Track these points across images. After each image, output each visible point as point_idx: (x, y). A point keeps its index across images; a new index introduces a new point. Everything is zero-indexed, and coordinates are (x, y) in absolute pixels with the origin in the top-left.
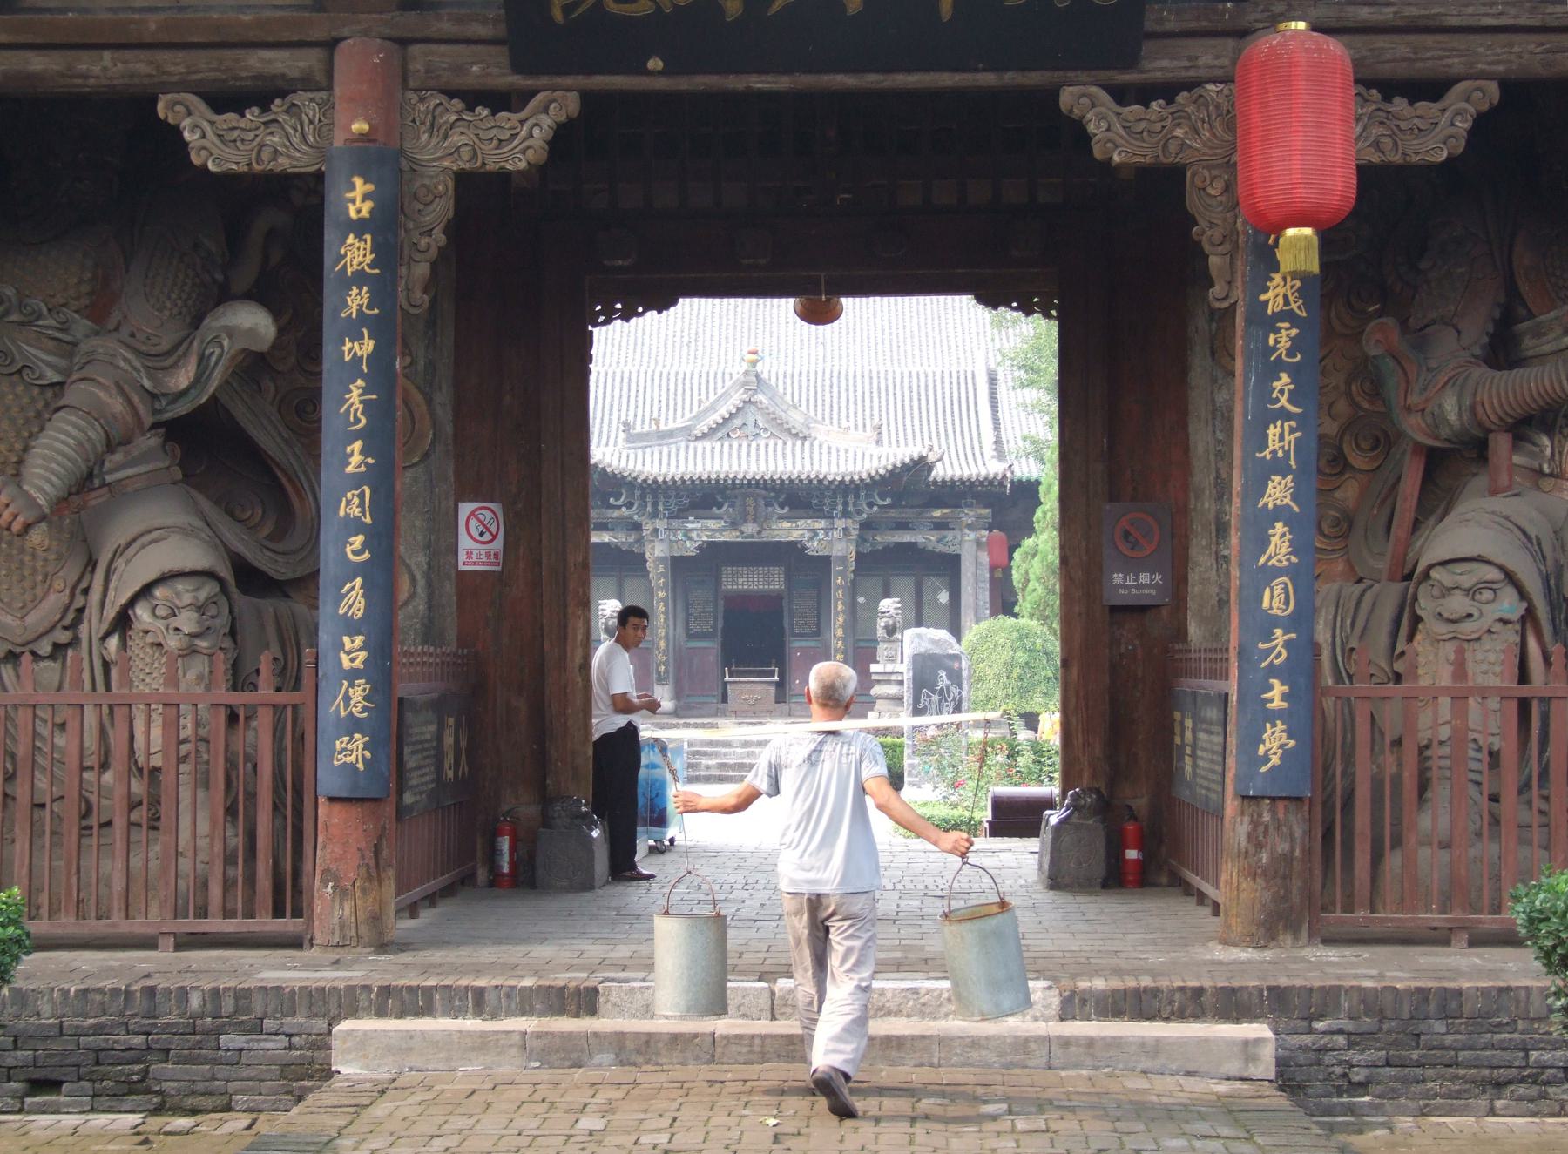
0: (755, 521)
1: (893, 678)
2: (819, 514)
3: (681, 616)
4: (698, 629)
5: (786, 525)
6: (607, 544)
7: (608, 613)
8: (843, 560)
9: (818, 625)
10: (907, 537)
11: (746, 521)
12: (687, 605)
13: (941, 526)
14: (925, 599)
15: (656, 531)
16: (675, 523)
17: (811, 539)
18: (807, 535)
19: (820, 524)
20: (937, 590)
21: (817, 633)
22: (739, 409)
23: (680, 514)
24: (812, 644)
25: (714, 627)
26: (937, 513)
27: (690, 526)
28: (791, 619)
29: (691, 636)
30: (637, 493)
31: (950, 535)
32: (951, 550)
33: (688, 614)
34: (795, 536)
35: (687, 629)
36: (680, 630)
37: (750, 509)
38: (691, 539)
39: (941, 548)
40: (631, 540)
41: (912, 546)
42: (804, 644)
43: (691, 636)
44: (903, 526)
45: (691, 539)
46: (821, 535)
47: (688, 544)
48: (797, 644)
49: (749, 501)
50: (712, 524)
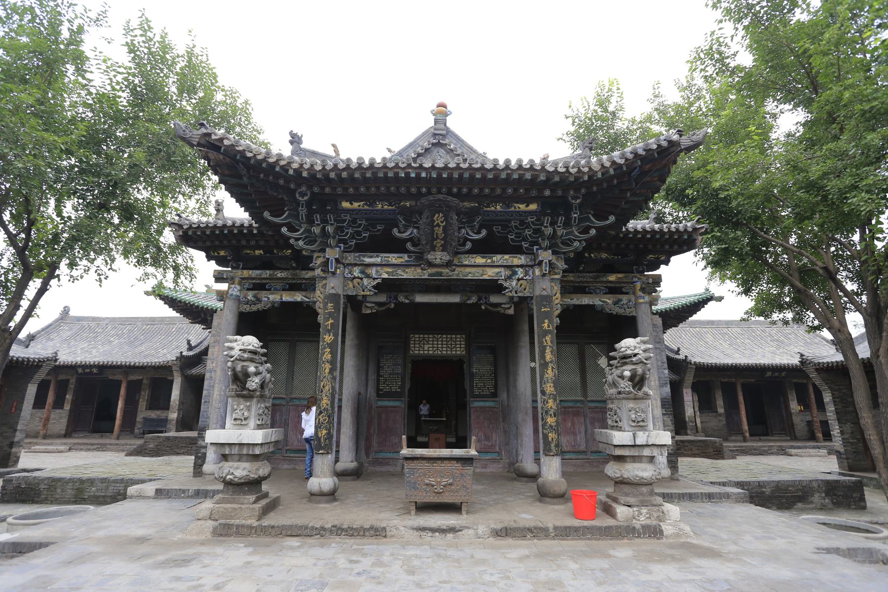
0: (444, 249)
1: (646, 452)
2: (517, 250)
3: (372, 377)
4: (387, 389)
5: (480, 260)
8: (547, 299)
9: (496, 387)
10: (586, 300)
11: (433, 249)
12: (379, 368)
13: (614, 290)
14: (587, 364)
15: (326, 263)
16: (351, 258)
17: (509, 278)
18: (504, 273)
20: (597, 357)
21: (495, 395)
22: (427, 150)
23: (362, 248)
24: (488, 404)
25: (402, 387)
26: (612, 278)
27: (368, 260)
28: (472, 382)
29: (380, 395)
30: (303, 211)
31: (624, 299)
32: (629, 312)
33: (379, 376)
34: (490, 274)
35: (378, 390)
36: (371, 391)
37: (439, 231)
38: (368, 276)
39: (616, 310)
41: (592, 307)
42: (481, 404)
43: (380, 395)
44: (582, 290)
45: (368, 276)
46: (520, 273)
47: (365, 281)
48: (476, 404)
49: (438, 218)
50: (393, 258)
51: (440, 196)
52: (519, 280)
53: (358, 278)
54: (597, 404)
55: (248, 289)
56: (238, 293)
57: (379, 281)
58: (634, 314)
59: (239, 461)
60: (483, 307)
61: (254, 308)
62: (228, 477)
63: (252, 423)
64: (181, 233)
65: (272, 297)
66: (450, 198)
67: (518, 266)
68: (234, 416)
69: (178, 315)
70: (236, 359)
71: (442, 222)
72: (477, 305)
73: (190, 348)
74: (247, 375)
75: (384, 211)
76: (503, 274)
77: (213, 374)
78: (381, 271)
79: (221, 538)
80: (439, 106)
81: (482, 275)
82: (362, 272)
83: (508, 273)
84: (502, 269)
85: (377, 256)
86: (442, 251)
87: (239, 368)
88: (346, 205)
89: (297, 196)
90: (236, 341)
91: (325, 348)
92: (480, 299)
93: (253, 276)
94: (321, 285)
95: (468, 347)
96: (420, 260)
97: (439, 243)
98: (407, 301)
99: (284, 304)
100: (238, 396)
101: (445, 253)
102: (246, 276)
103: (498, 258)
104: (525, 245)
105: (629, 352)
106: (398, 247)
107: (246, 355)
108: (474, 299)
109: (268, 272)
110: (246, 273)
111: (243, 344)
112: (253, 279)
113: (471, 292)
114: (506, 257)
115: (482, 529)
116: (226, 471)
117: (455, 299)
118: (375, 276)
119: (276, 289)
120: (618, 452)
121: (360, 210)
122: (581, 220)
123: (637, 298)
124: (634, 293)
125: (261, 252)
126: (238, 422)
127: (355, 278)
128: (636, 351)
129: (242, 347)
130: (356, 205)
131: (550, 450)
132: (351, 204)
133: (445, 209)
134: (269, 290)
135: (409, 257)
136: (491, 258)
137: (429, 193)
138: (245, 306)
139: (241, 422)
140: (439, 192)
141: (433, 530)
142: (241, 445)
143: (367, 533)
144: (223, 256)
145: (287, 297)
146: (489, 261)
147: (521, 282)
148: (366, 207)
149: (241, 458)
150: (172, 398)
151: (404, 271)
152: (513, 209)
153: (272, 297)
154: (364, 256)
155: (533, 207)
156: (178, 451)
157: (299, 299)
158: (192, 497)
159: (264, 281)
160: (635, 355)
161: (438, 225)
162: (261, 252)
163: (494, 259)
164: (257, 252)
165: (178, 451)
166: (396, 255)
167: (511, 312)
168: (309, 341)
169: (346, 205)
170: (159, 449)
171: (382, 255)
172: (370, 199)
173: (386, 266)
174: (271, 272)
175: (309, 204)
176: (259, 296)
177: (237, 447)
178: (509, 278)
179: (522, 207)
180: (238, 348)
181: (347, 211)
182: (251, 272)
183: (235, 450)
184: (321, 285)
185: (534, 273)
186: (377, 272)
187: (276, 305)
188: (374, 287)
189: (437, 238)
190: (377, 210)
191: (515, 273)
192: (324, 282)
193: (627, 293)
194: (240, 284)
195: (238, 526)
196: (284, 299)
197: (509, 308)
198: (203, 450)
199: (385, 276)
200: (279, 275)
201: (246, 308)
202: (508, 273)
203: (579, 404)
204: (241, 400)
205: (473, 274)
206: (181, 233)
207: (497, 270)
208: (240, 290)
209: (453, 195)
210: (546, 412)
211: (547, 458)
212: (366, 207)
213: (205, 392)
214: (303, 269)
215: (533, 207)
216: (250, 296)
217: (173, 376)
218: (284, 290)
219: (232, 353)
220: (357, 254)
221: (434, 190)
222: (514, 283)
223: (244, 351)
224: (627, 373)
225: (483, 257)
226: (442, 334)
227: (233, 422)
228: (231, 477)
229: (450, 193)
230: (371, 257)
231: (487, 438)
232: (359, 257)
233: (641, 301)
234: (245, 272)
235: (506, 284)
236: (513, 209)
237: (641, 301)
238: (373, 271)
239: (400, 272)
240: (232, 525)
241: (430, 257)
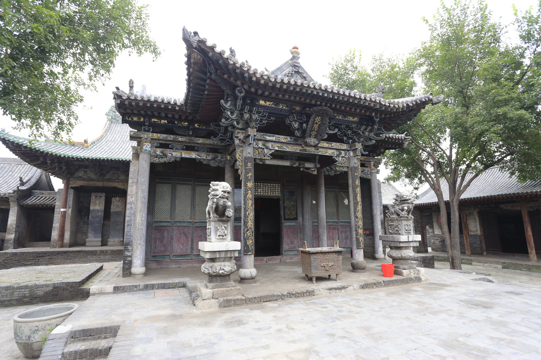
6: (194, 160)
7: (220, 193)
9: (297, 214)
17: (338, 156)
18: (336, 153)
19: (345, 147)
21: (296, 219)
27: (268, 138)
28: (284, 211)
30: (239, 103)
31: (366, 169)
34: (329, 153)
37: (316, 126)
38: (267, 148)
40: (209, 158)
42: (289, 224)
45: (267, 148)
47: (266, 151)
48: (286, 224)
49: (318, 119)
50: (282, 138)
51: (325, 108)
52: (342, 157)
53: (261, 148)
54: (343, 224)
55: (156, 147)
56: (150, 150)
57: (273, 151)
58: (370, 178)
59: (224, 261)
60: (301, 169)
61: (162, 160)
62: (221, 272)
63: (229, 237)
64: (119, 102)
65: (174, 154)
66: (329, 109)
67: (342, 150)
68: (218, 233)
69: (17, 157)
70: (220, 197)
72: (298, 168)
73: (22, 184)
74: (225, 207)
75: (282, 109)
76: (335, 153)
77: (133, 205)
78: (275, 146)
79: (225, 308)
80: (293, 48)
81: (326, 153)
82: (264, 145)
83: (338, 153)
84: (335, 151)
85: (273, 136)
86: (314, 138)
87: (221, 202)
88: (262, 102)
89: (237, 92)
90: (217, 185)
91: (248, 191)
92: (300, 165)
93: (161, 138)
94: (239, 150)
95: (282, 191)
96: (296, 141)
97: (314, 133)
98: (261, 163)
99: (182, 159)
100: (219, 221)
101: (315, 139)
102: (156, 137)
103: (335, 145)
104: (345, 138)
105: (408, 198)
106: (287, 131)
107: (226, 195)
108: (297, 165)
109: (172, 136)
110: (155, 136)
111: (223, 188)
112: (160, 140)
113: (296, 160)
114: (338, 144)
115: (356, 286)
116: (218, 268)
117: (287, 163)
118: (271, 148)
119: (177, 149)
120: (402, 245)
121: (269, 107)
122: (378, 129)
123: (371, 170)
124: (370, 167)
125: (166, 121)
126: (221, 237)
127: (259, 148)
128: (410, 198)
129: (224, 190)
130: (268, 103)
131: (360, 246)
132: (265, 102)
133: (322, 114)
134: (172, 149)
135: (291, 138)
136: (331, 144)
137: (320, 105)
138: (155, 159)
139: (222, 237)
140: (326, 106)
141: (336, 289)
142: (226, 251)
143: (305, 295)
144: (135, 121)
145: (186, 155)
147: (344, 158)
148: (273, 106)
149: (225, 259)
150: (9, 222)
151: (287, 147)
152: (346, 119)
153: (174, 154)
154: (266, 135)
155: (356, 119)
156: (26, 263)
157: (194, 157)
158: (142, 290)
159: (168, 142)
160: (410, 199)
161: (317, 123)
162: (166, 121)
163: (333, 145)
164: (163, 121)
165: (26, 263)
166: (284, 137)
167: (315, 173)
168: (185, 184)
169: (262, 102)
170: (6, 263)
171: (276, 136)
172: (277, 101)
173: (277, 142)
174: (174, 136)
175: (244, 99)
176: (165, 152)
177: (224, 253)
178: (338, 156)
179: (351, 119)
180: (221, 190)
181: (262, 106)
182: (159, 135)
183: (223, 255)
184: (239, 150)
185: (349, 153)
186: (272, 145)
187: (178, 159)
189: (314, 130)
190: (279, 109)
191: (341, 153)
192: (241, 149)
193: (367, 167)
194: (150, 143)
195: (235, 300)
196: (183, 156)
197: (314, 171)
198: (129, 259)
199: (277, 149)
200: (180, 139)
201: (157, 160)
202: (338, 153)
203: (335, 224)
204: (221, 223)
205: (322, 152)
206: (119, 102)
207: (332, 151)
208: (151, 147)
209: (332, 109)
210: (358, 227)
211: (358, 250)
212: (273, 106)
213: (127, 219)
214: (196, 137)
215: (356, 119)
216: (158, 151)
217: (9, 205)
218: (183, 149)
219: (217, 193)
220: (262, 134)
221: (324, 104)
222: (340, 159)
223: (225, 192)
224: (406, 208)
225: (327, 143)
226: (268, 183)
227: (218, 237)
228: (223, 271)
229: (330, 107)
230: (270, 136)
231: (292, 243)
232: (263, 135)
233: (373, 171)
234: (155, 134)
235: (337, 159)
236: (346, 119)
237: (373, 171)
238: (270, 145)
239: (284, 147)
240: (231, 300)
241: (308, 140)
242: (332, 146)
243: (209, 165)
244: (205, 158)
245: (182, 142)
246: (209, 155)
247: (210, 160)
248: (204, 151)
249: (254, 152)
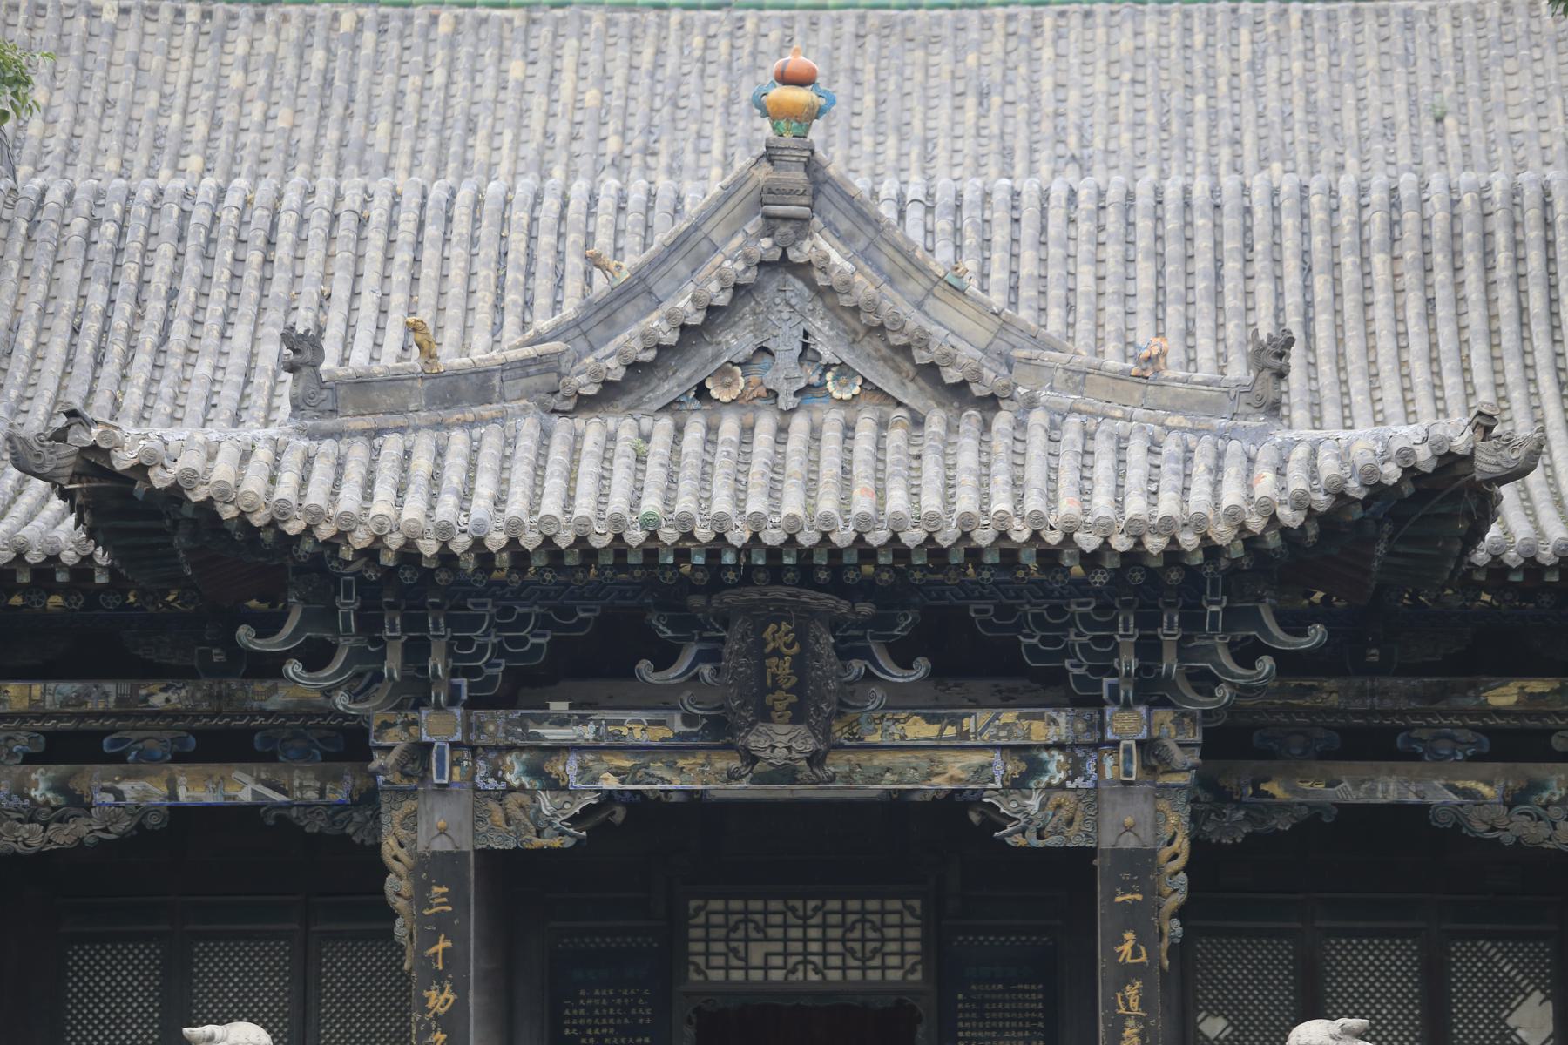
6: (249, 813)
34: (955, 770)
47: (546, 803)
53: (522, 789)
71: (789, 646)
76: (998, 771)
78: (597, 768)
81: (929, 776)
82: (534, 771)
136: (955, 721)
146: (950, 731)
151: (671, 766)
157: (245, 796)
163: (968, 724)
166: (644, 717)
178: (1018, 784)
186: (583, 769)
188: (574, 820)
196: (184, 795)
199: (611, 783)
200: (158, 700)
218: (179, 758)
239: (657, 768)
242: (964, 735)
243: (347, 838)
244: (312, 795)
245: (175, 715)
246: (337, 778)
247: (341, 807)
248: (306, 756)
249: (477, 819)
